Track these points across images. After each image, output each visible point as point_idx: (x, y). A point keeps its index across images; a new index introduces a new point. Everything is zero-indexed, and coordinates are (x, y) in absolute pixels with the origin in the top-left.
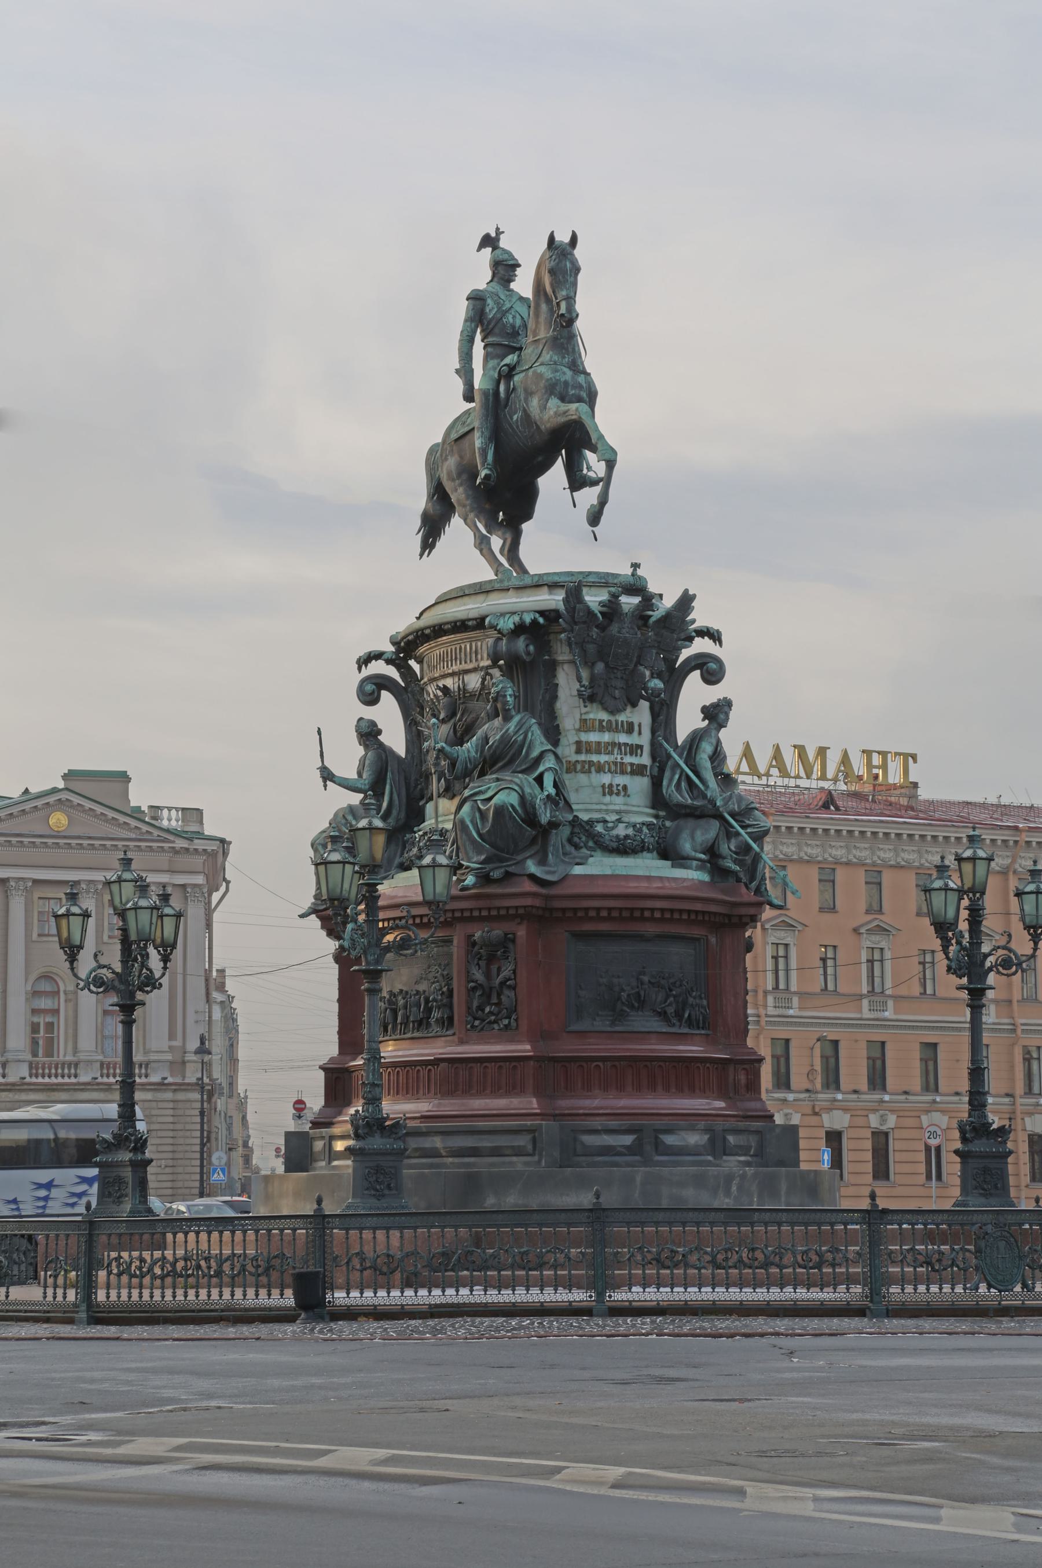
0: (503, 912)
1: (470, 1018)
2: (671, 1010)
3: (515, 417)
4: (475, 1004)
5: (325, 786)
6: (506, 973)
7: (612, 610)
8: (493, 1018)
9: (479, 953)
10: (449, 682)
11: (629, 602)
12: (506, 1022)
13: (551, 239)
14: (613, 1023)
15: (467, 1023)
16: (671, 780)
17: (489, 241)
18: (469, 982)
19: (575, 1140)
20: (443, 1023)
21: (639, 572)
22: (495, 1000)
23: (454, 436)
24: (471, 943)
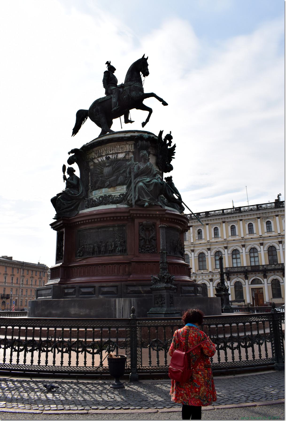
0: (151, 216)
1: (140, 249)
3: (124, 97)
4: (142, 244)
5: (64, 181)
6: (153, 235)
8: (148, 249)
9: (143, 228)
10: (110, 156)
12: (153, 250)
13: (144, 56)
14: (175, 254)
15: (139, 250)
16: (169, 192)
18: (140, 237)
19: (181, 288)
20: (123, 251)
22: (148, 243)
24: (141, 224)
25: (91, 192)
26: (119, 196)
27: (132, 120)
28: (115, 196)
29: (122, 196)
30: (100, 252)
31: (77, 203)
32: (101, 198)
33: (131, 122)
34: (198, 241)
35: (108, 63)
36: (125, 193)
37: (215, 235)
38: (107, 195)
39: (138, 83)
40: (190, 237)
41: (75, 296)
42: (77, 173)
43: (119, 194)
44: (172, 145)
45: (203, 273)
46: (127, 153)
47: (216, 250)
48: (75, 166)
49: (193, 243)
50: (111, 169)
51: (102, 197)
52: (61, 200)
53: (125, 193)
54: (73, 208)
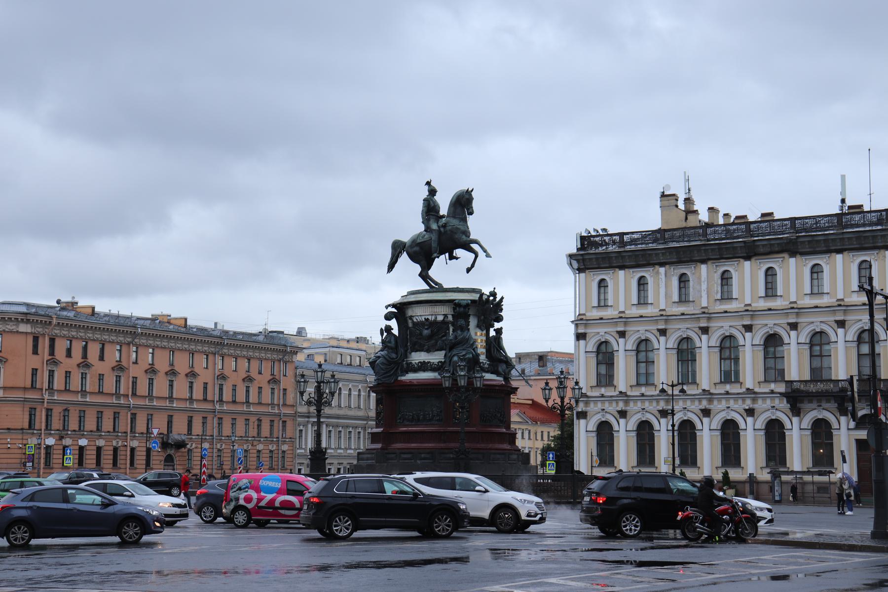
2: (502, 419)
7: (488, 300)
11: (491, 298)
16: (494, 351)
17: (428, 183)
21: (495, 291)
23: (419, 241)
25: (410, 353)
26: (438, 363)
27: (458, 257)
28: (433, 363)
29: (440, 364)
30: (419, 420)
31: (396, 367)
32: (420, 364)
33: (457, 258)
34: (720, 305)
35: (428, 183)
36: (443, 360)
37: (766, 289)
38: (426, 361)
39: (461, 223)
40: (700, 291)
41: (396, 461)
42: (395, 331)
43: (438, 361)
44: (498, 300)
45: (730, 392)
46: (446, 316)
47: (768, 332)
48: (393, 323)
49: (706, 308)
50: (430, 332)
51: (421, 362)
52: (381, 366)
53: (443, 360)
54: (392, 372)
